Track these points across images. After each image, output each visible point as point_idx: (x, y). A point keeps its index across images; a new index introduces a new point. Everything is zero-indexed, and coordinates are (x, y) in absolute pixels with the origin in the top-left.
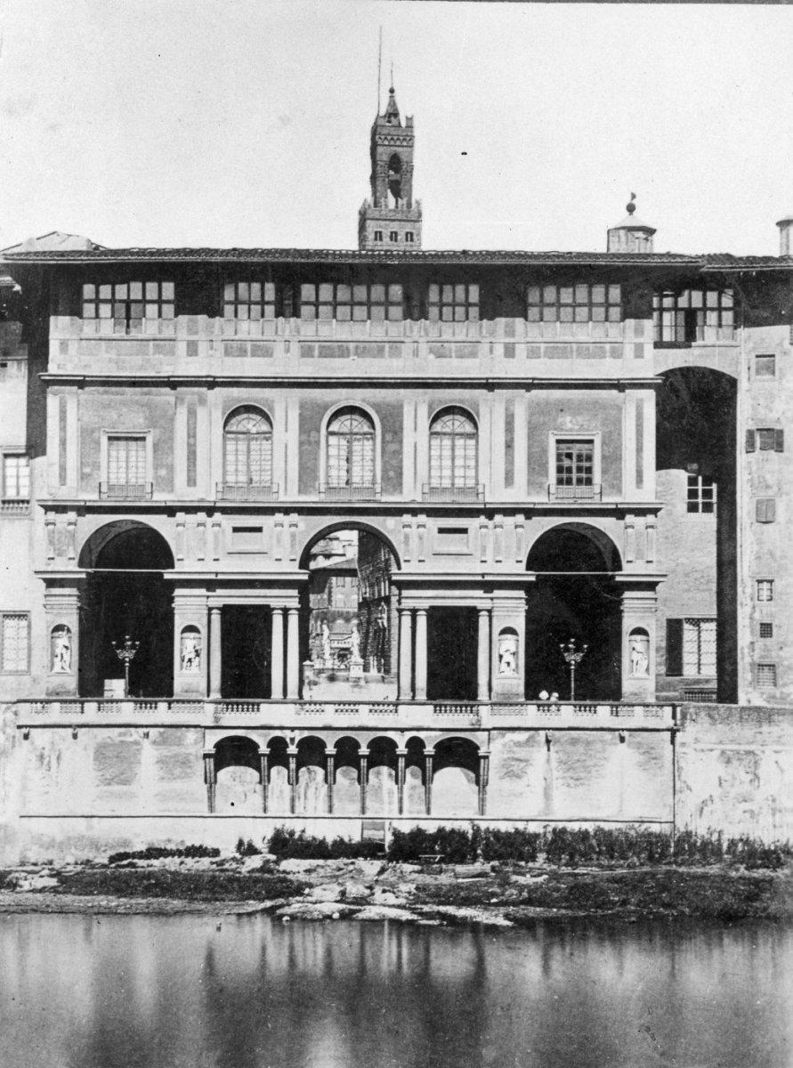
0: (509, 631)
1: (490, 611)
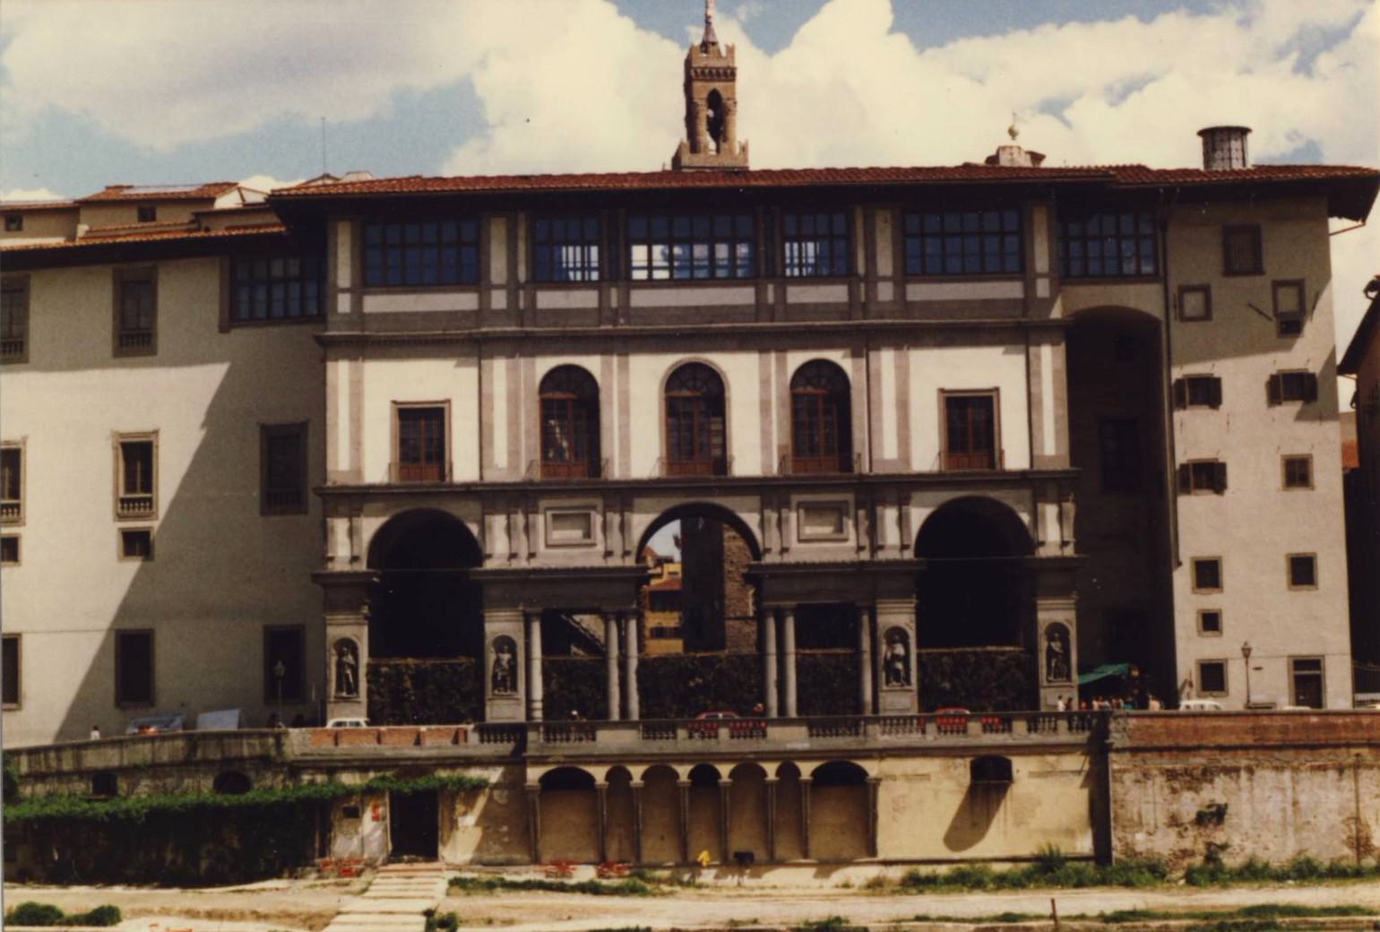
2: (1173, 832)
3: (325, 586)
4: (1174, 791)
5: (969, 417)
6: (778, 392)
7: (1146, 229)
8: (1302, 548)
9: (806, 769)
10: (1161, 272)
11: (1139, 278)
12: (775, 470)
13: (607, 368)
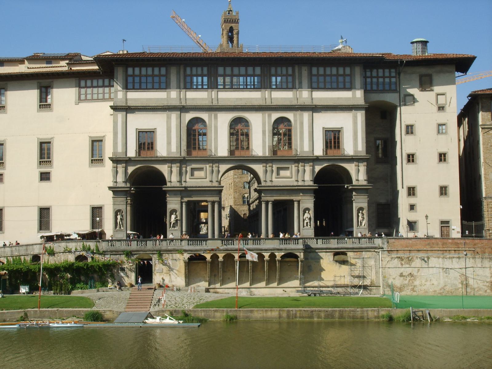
0: (308, 209)
1: (299, 202)
2: (402, 278)
3: (113, 191)
4: (402, 264)
5: (333, 139)
6: (268, 129)
7: (393, 74)
8: (443, 184)
9: (279, 255)
10: (398, 90)
11: (391, 91)
12: (267, 155)
13: (210, 118)
